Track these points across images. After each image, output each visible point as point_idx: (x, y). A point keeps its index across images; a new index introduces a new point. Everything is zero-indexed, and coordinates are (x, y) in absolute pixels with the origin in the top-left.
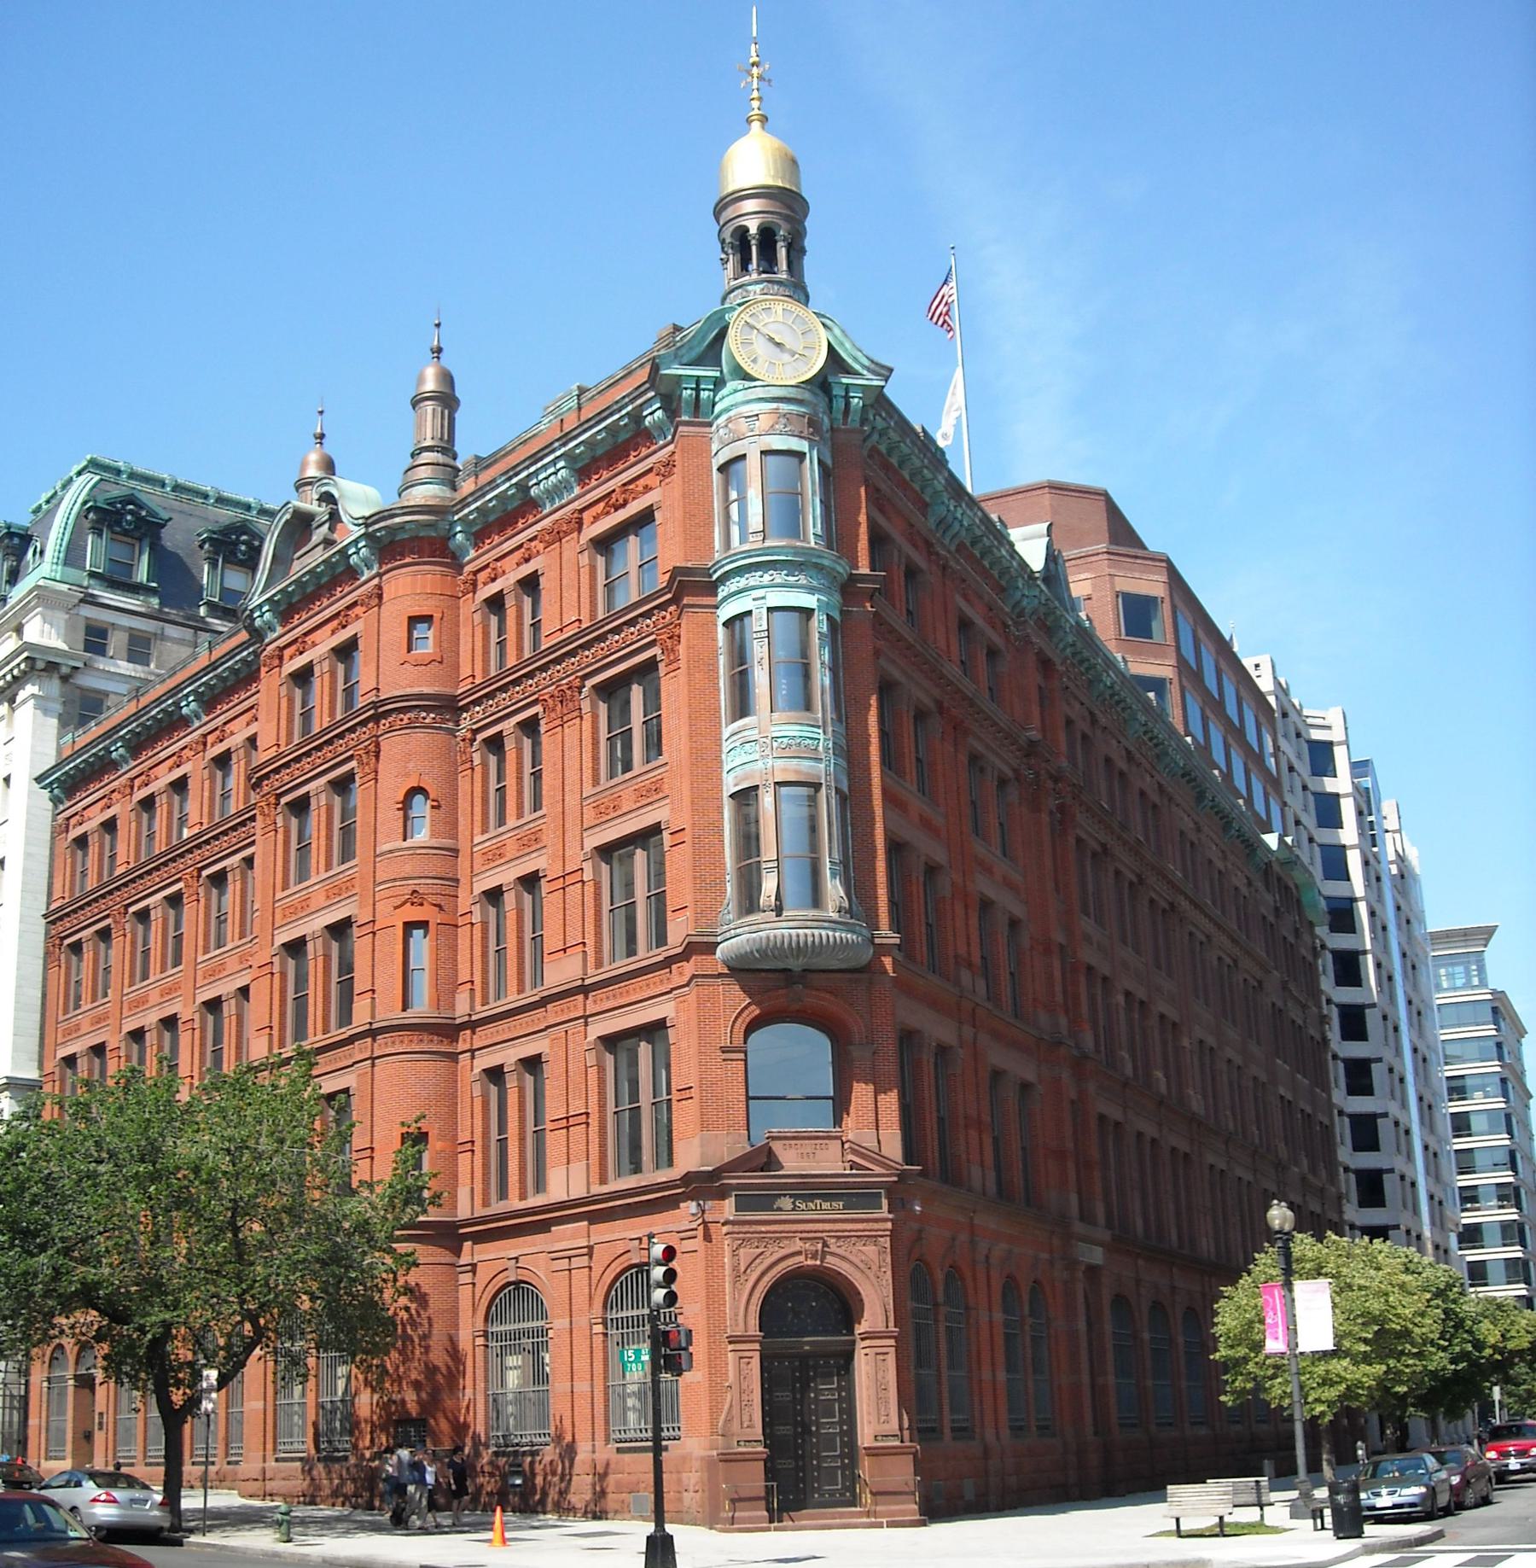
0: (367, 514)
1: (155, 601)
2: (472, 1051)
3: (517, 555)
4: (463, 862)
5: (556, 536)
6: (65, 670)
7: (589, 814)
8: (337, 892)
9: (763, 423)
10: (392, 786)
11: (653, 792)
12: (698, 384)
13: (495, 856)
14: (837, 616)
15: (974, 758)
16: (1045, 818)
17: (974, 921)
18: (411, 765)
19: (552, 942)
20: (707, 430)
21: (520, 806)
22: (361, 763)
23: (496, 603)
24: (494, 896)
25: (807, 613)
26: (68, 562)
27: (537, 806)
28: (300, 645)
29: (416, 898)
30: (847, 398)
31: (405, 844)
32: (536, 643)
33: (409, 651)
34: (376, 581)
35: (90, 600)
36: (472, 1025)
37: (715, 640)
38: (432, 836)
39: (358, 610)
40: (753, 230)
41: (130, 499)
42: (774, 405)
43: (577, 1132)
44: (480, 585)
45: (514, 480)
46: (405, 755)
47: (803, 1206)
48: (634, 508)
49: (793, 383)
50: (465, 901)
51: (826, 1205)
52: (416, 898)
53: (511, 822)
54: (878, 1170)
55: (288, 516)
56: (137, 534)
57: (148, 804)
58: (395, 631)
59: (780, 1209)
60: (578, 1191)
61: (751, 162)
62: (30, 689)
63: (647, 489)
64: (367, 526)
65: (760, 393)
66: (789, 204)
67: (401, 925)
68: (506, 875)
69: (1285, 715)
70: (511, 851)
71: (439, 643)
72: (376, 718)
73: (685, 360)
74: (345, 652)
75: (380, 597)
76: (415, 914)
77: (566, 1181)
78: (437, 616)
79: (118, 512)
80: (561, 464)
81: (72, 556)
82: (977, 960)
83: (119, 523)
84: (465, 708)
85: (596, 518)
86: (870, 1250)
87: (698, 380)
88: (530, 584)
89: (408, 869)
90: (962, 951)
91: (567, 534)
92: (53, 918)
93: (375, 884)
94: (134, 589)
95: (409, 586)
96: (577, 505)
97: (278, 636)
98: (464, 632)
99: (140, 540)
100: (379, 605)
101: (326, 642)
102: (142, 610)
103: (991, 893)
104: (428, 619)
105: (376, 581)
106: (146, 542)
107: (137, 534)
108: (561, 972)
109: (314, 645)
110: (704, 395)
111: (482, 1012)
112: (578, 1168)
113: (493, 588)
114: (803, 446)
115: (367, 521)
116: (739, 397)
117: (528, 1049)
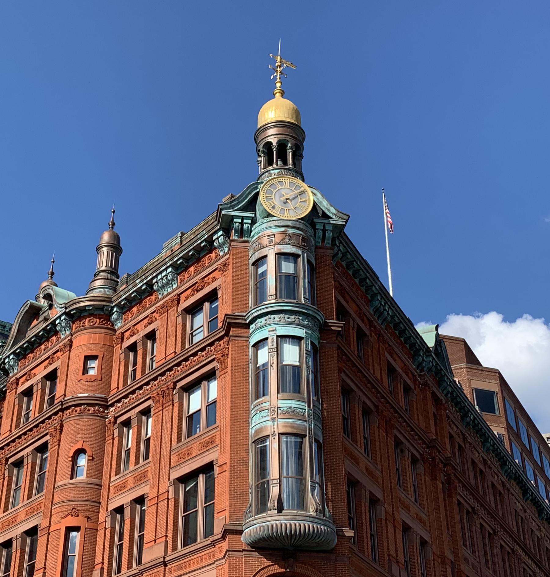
0: (66, 302)
3: (146, 321)
4: (104, 493)
5: (165, 309)
8: (31, 512)
9: (278, 239)
10: (67, 449)
11: (210, 444)
12: (242, 221)
13: (122, 488)
15: (398, 443)
16: (440, 485)
17: (399, 535)
18: (79, 436)
19: (149, 535)
20: (247, 245)
22: (52, 436)
23: (133, 348)
24: (120, 510)
27: (147, 457)
28: (28, 375)
29: (74, 512)
30: (324, 230)
33: (83, 374)
37: (247, 355)
38: (87, 476)
39: (59, 354)
40: (274, 143)
42: (283, 229)
44: (125, 339)
45: (145, 281)
48: (207, 290)
49: (294, 219)
50: (103, 516)
53: (132, 467)
55: (27, 308)
58: (77, 364)
61: (274, 112)
63: (214, 279)
64: (66, 308)
65: (276, 223)
66: (294, 131)
68: (124, 499)
70: (130, 485)
71: (100, 369)
72: (62, 410)
74: (52, 377)
75: (71, 346)
76: (71, 521)
78: (101, 356)
80: (169, 270)
82: (401, 559)
84: (112, 405)
85: (187, 298)
87: (243, 218)
88: (151, 336)
90: (392, 552)
91: (171, 307)
97: (15, 373)
98: (115, 365)
101: (41, 372)
103: (409, 522)
104: (94, 358)
109: (35, 375)
110: (246, 226)
116: (264, 226)
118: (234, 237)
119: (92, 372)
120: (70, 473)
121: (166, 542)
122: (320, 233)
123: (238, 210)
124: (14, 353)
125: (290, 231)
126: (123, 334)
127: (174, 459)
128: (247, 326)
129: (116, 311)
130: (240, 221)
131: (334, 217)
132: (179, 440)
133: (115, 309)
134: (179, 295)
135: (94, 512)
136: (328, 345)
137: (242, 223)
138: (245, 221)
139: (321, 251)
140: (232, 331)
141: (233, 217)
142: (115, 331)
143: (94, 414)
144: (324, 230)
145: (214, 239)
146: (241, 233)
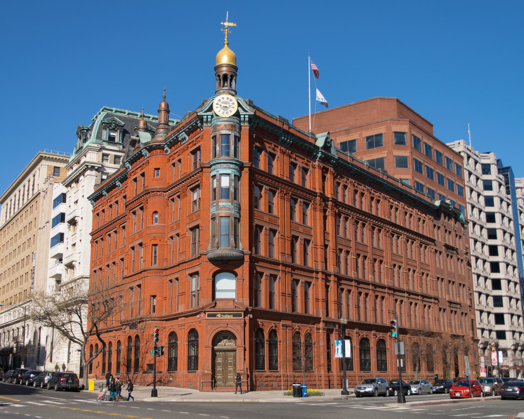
1: (121, 147)
3: (177, 154)
5: (184, 150)
6: (96, 168)
7: (188, 220)
13: (172, 228)
26: (97, 139)
30: (244, 118)
46: (154, 203)
50: (166, 239)
51: (229, 316)
57: (111, 206)
62: (88, 172)
63: (200, 141)
68: (173, 234)
69: (469, 157)
70: (175, 228)
76: (154, 242)
79: (110, 123)
81: (99, 136)
83: (111, 126)
85: (191, 147)
87: (207, 116)
92: (92, 234)
94: (116, 144)
102: (118, 149)
110: (209, 120)
113: (173, 161)
114: (230, 132)
117: (176, 277)
118: (205, 125)
124: (128, 161)
125: (226, 123)
137: (207, 118)
140: (204, 169)
141: (203, 116)
144: (244, 118)
146: (207, 122)
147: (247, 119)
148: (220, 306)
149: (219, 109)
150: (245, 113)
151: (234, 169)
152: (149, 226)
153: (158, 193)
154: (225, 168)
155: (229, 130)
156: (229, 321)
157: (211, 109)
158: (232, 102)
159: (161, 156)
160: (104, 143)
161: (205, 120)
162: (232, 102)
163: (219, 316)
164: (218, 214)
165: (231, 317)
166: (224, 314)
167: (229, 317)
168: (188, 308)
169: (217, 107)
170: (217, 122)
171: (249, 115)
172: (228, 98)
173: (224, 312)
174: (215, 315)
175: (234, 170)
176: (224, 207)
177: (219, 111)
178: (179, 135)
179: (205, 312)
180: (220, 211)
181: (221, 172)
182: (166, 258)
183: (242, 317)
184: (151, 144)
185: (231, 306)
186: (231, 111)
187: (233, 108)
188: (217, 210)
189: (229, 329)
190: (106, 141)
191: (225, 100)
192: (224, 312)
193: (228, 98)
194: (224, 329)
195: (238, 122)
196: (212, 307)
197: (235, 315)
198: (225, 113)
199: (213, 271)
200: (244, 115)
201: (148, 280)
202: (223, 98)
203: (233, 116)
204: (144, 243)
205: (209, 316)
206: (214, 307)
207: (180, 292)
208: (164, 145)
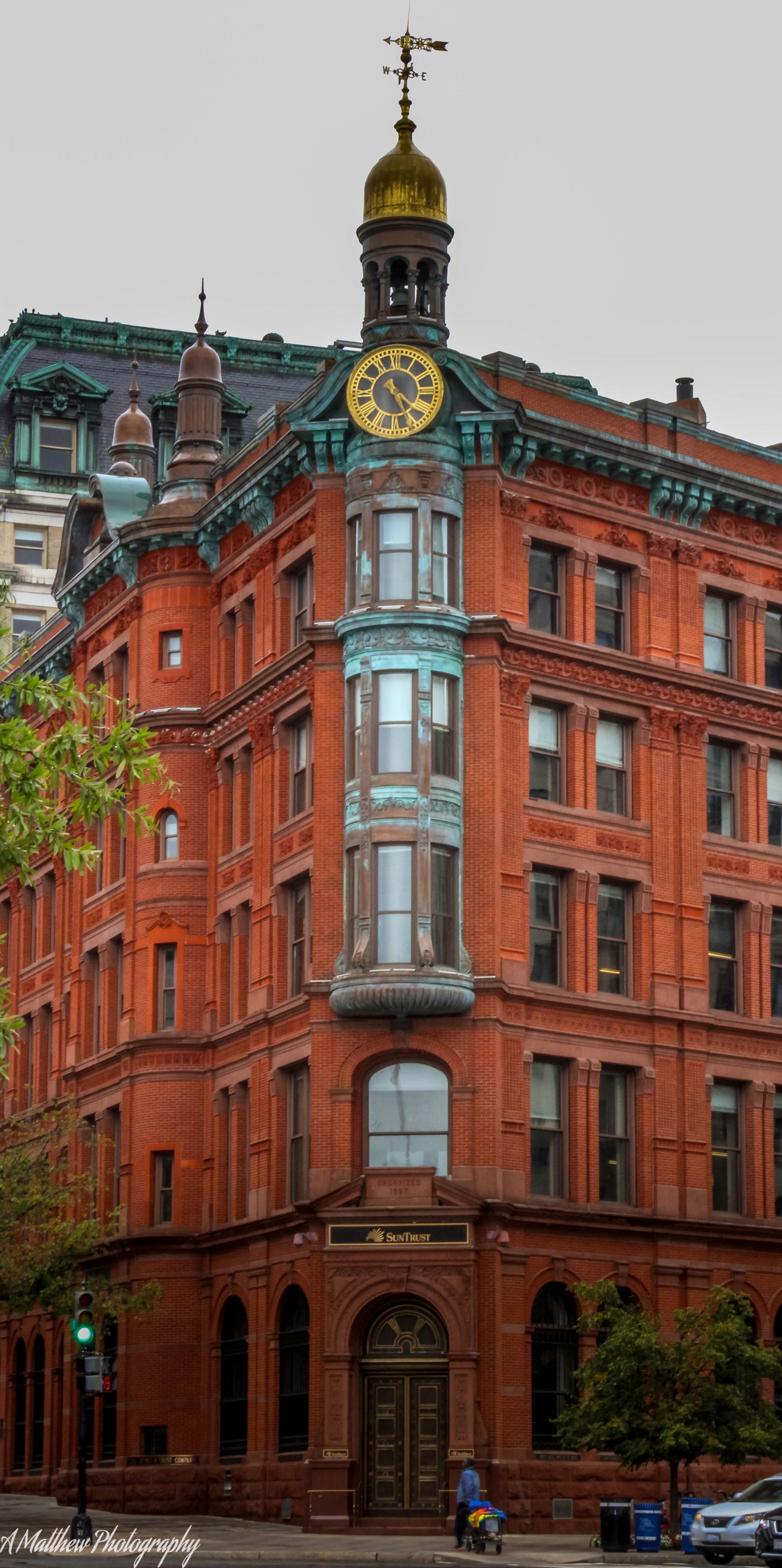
2: (213, 1071)
14: (453, 668)
21: (229, 837)
25: (414, 672)
29: (164, 920)
30: (477, 435)
31: (157, 866)
32: (247, 670)
33: (161, 666)
34: (135, 592)
35: (18, 504)
36: (211, 1046)
37: (341, 697)
41: (61, 378)
42: (384, 463)
43: (264, 1156)
47: (393, 1238)
50: (211, 922)
51: (414, 1237)
52: (164, 920)
54: (462, 1205)
56: (71, 414)
58: (149, 650)
59: (371, 1241)
60: (263, 1215)
67: (151, 947)
68: (231, 901)
73: (315, 415)
75: (139, 608)
76: (162, 935)
77: (258, 1206)
79: (46, 393)
80: (256, 493)
86: (454, 1280)
89: (159, 891)
93: (136, 905)
95: (163, 601)
96: (272, 534)
99: (75, 421)
100: (139, 617)
104: (177, 633)
105: (135, 592)
106: (83, 424)
107: (71, 414)
108: (258, 1002)
110: (336, 449)
111: (224, 1032)
112: (263, 1190)
114: (414, 502)
115: (122, 532)
119: (176, 660)
120: (153, 852)
121: (270, 988)
122: (470, 439)
123: (322, 417)
126: (220, 585)
127: (277, 851)
128: (340, 642)
129: (205, 541)
130: (323, 438)
131: (493, 407)
132: (284, 817)
133: (202, 538)
134: (275, 541)
135: (197, 916)
136: (479, 662)
137: (329, 443)
138: (334, 438)
139: (477, 474)
141: (311, 434)
142: (210, 575)
143: (187, 741)
144: (477, 435)
145: (299, 458)
146: (330, 458)
147: (487, 440)
148: (382, 1196)
149: (372, 405)
150: (476, 416)
151: (429, 648)
152: (142, 868)
153: (177, 734)
154: (395, 648)
155: (408, 491)
156: (415, 1257)
157: (338, 406)
158: (422, 376)
159: (186, 579)
160: (20, 480)
161: (319, 449)
162: (422, 376)
163: (378, 1236)
164: (370, 833)
165: (422, 1242)
166: (397, 1231)
167: (415, 1241)
168: (280, 1205)
169: (362, 401)
170: (362, 460)
171: (496, 425)
172: (405, 361)
173: (396, 1221)
174: (360, 1235)
175: (428, 655)
176: (391, 806)
177: (372, 417)
178: (242, 497)
179: (322, 1224)
180: (374, 823)
181: (377, 664)
182: (209, 998)
183: (468, 1243)
184: (144, 534)
185: (419, 1197)
186: (418, 414)
187: (427, 398)
188: (363, 820)
189: (417, 1290)
190: (30, 473)
191: (395, 366)
192: (396, 1221)
193: (405, 361)
194: (395, 1290)
195: (452, 454)
196: (348, 1204)
197: (437, 1234)
198: (395, 422)
199: (355, 1061)
200: (477, 426)
201: (142, 1089)
202: (386, 361)
203: (429, 429)
204: (127, 939)
205: (338, 1236)
206: (357, 1202)
207: (254, 1139)
208: (197, 535)
